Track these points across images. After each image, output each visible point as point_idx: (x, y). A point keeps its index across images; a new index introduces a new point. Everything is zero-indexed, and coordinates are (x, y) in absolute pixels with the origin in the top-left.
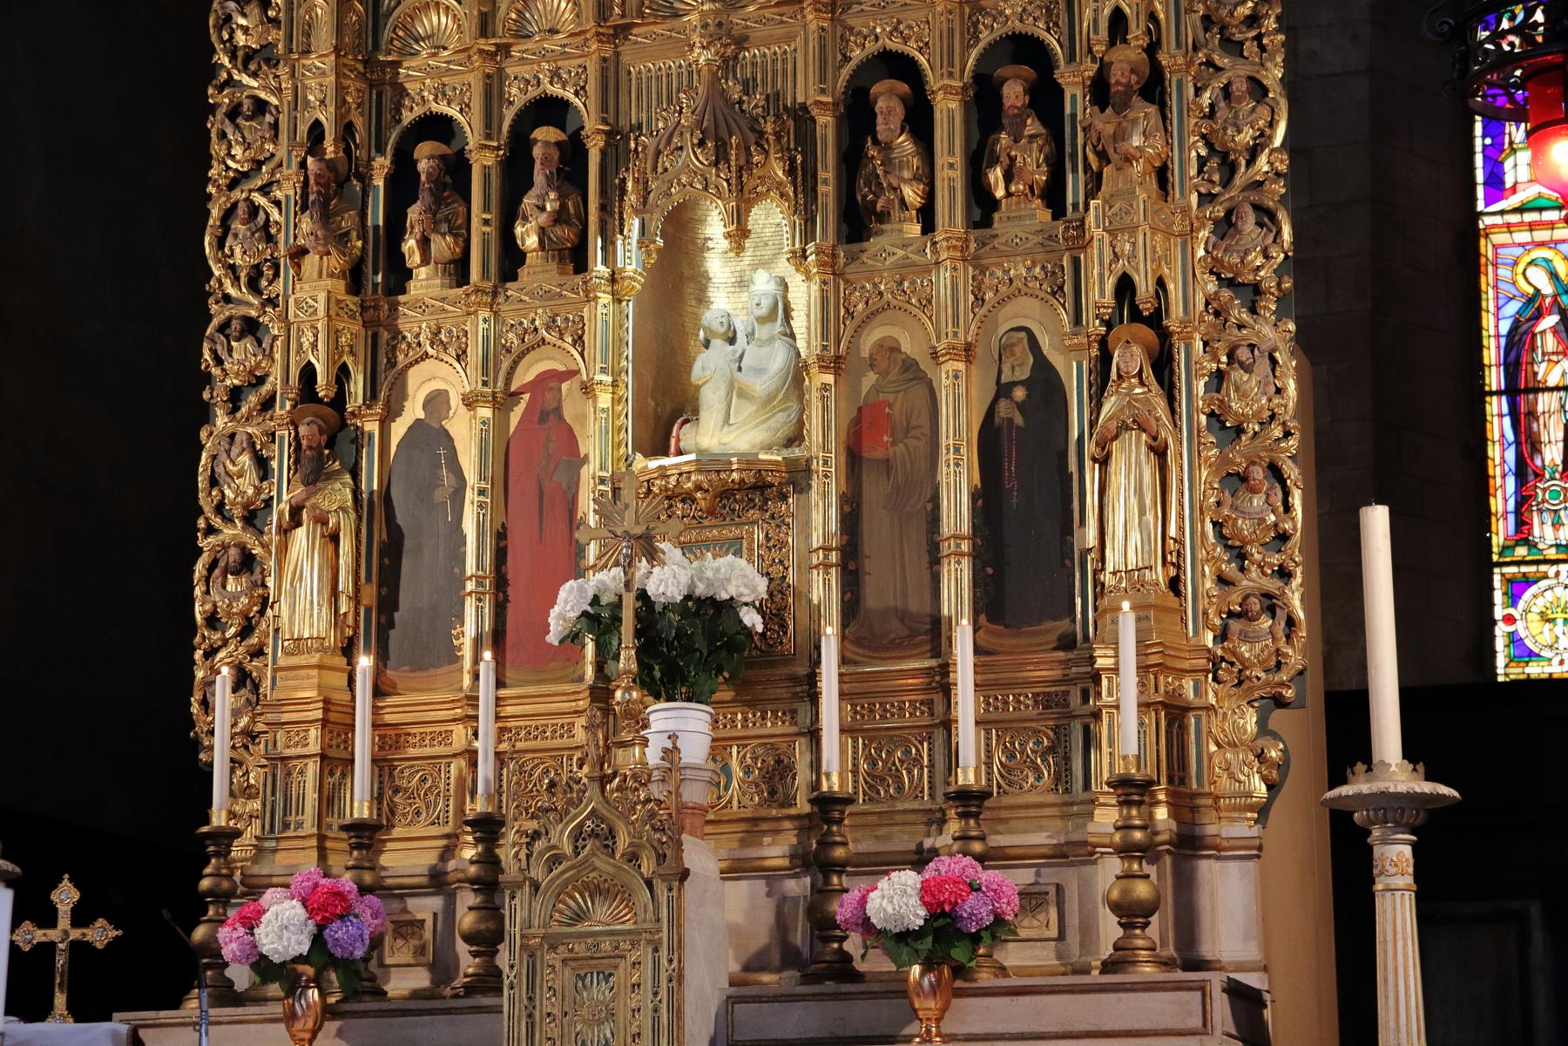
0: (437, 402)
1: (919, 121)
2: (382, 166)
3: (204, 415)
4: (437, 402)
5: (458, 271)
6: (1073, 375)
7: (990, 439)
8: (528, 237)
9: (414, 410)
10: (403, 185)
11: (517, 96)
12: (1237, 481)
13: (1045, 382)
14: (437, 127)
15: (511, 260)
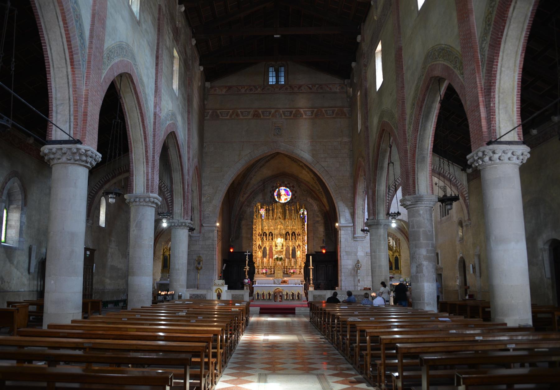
0: (265, 246)
1: (289, 235)
2: (262, 234)
3: (253, 245)
4: (265, 246)
5: (266, 239)
6: (296, 247)
7: (292, 250)
8: (270, 238)
9: (264, 246)
10: (263, 235)
11: (269, 232)
12: (303, 253)
13: (295, 248)
14: (265, 232)
15: (269, 239)
